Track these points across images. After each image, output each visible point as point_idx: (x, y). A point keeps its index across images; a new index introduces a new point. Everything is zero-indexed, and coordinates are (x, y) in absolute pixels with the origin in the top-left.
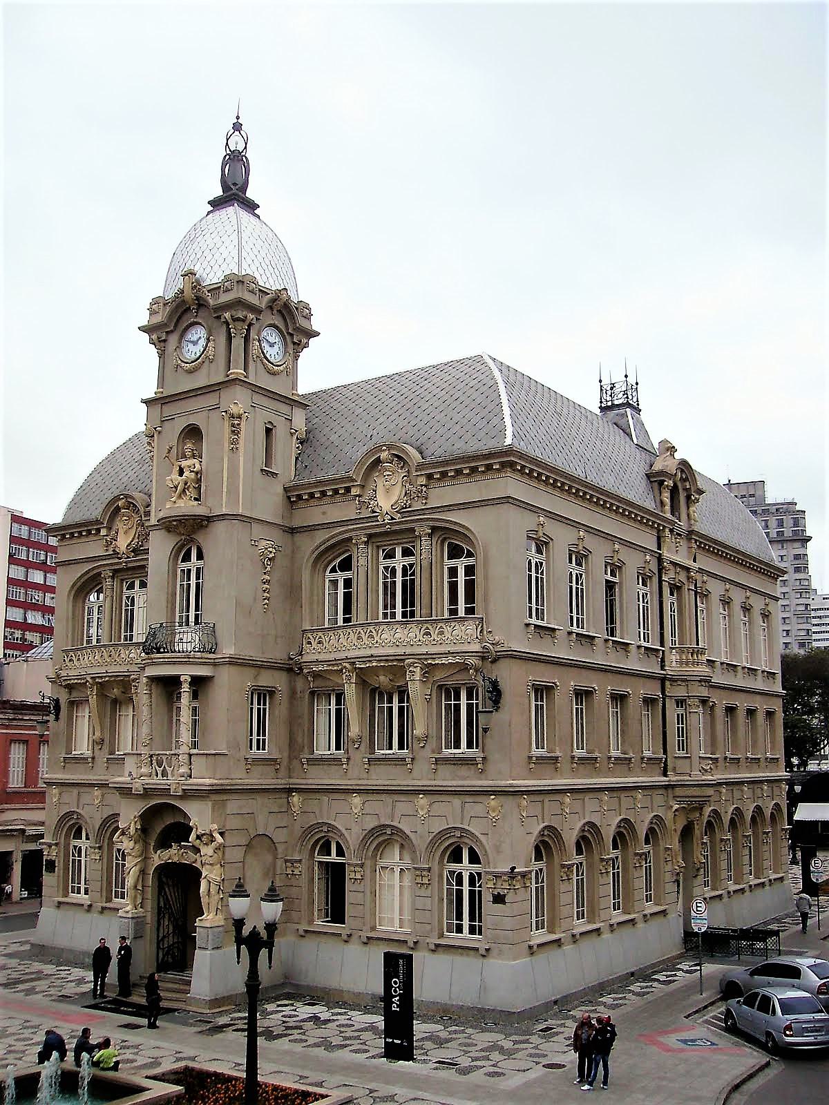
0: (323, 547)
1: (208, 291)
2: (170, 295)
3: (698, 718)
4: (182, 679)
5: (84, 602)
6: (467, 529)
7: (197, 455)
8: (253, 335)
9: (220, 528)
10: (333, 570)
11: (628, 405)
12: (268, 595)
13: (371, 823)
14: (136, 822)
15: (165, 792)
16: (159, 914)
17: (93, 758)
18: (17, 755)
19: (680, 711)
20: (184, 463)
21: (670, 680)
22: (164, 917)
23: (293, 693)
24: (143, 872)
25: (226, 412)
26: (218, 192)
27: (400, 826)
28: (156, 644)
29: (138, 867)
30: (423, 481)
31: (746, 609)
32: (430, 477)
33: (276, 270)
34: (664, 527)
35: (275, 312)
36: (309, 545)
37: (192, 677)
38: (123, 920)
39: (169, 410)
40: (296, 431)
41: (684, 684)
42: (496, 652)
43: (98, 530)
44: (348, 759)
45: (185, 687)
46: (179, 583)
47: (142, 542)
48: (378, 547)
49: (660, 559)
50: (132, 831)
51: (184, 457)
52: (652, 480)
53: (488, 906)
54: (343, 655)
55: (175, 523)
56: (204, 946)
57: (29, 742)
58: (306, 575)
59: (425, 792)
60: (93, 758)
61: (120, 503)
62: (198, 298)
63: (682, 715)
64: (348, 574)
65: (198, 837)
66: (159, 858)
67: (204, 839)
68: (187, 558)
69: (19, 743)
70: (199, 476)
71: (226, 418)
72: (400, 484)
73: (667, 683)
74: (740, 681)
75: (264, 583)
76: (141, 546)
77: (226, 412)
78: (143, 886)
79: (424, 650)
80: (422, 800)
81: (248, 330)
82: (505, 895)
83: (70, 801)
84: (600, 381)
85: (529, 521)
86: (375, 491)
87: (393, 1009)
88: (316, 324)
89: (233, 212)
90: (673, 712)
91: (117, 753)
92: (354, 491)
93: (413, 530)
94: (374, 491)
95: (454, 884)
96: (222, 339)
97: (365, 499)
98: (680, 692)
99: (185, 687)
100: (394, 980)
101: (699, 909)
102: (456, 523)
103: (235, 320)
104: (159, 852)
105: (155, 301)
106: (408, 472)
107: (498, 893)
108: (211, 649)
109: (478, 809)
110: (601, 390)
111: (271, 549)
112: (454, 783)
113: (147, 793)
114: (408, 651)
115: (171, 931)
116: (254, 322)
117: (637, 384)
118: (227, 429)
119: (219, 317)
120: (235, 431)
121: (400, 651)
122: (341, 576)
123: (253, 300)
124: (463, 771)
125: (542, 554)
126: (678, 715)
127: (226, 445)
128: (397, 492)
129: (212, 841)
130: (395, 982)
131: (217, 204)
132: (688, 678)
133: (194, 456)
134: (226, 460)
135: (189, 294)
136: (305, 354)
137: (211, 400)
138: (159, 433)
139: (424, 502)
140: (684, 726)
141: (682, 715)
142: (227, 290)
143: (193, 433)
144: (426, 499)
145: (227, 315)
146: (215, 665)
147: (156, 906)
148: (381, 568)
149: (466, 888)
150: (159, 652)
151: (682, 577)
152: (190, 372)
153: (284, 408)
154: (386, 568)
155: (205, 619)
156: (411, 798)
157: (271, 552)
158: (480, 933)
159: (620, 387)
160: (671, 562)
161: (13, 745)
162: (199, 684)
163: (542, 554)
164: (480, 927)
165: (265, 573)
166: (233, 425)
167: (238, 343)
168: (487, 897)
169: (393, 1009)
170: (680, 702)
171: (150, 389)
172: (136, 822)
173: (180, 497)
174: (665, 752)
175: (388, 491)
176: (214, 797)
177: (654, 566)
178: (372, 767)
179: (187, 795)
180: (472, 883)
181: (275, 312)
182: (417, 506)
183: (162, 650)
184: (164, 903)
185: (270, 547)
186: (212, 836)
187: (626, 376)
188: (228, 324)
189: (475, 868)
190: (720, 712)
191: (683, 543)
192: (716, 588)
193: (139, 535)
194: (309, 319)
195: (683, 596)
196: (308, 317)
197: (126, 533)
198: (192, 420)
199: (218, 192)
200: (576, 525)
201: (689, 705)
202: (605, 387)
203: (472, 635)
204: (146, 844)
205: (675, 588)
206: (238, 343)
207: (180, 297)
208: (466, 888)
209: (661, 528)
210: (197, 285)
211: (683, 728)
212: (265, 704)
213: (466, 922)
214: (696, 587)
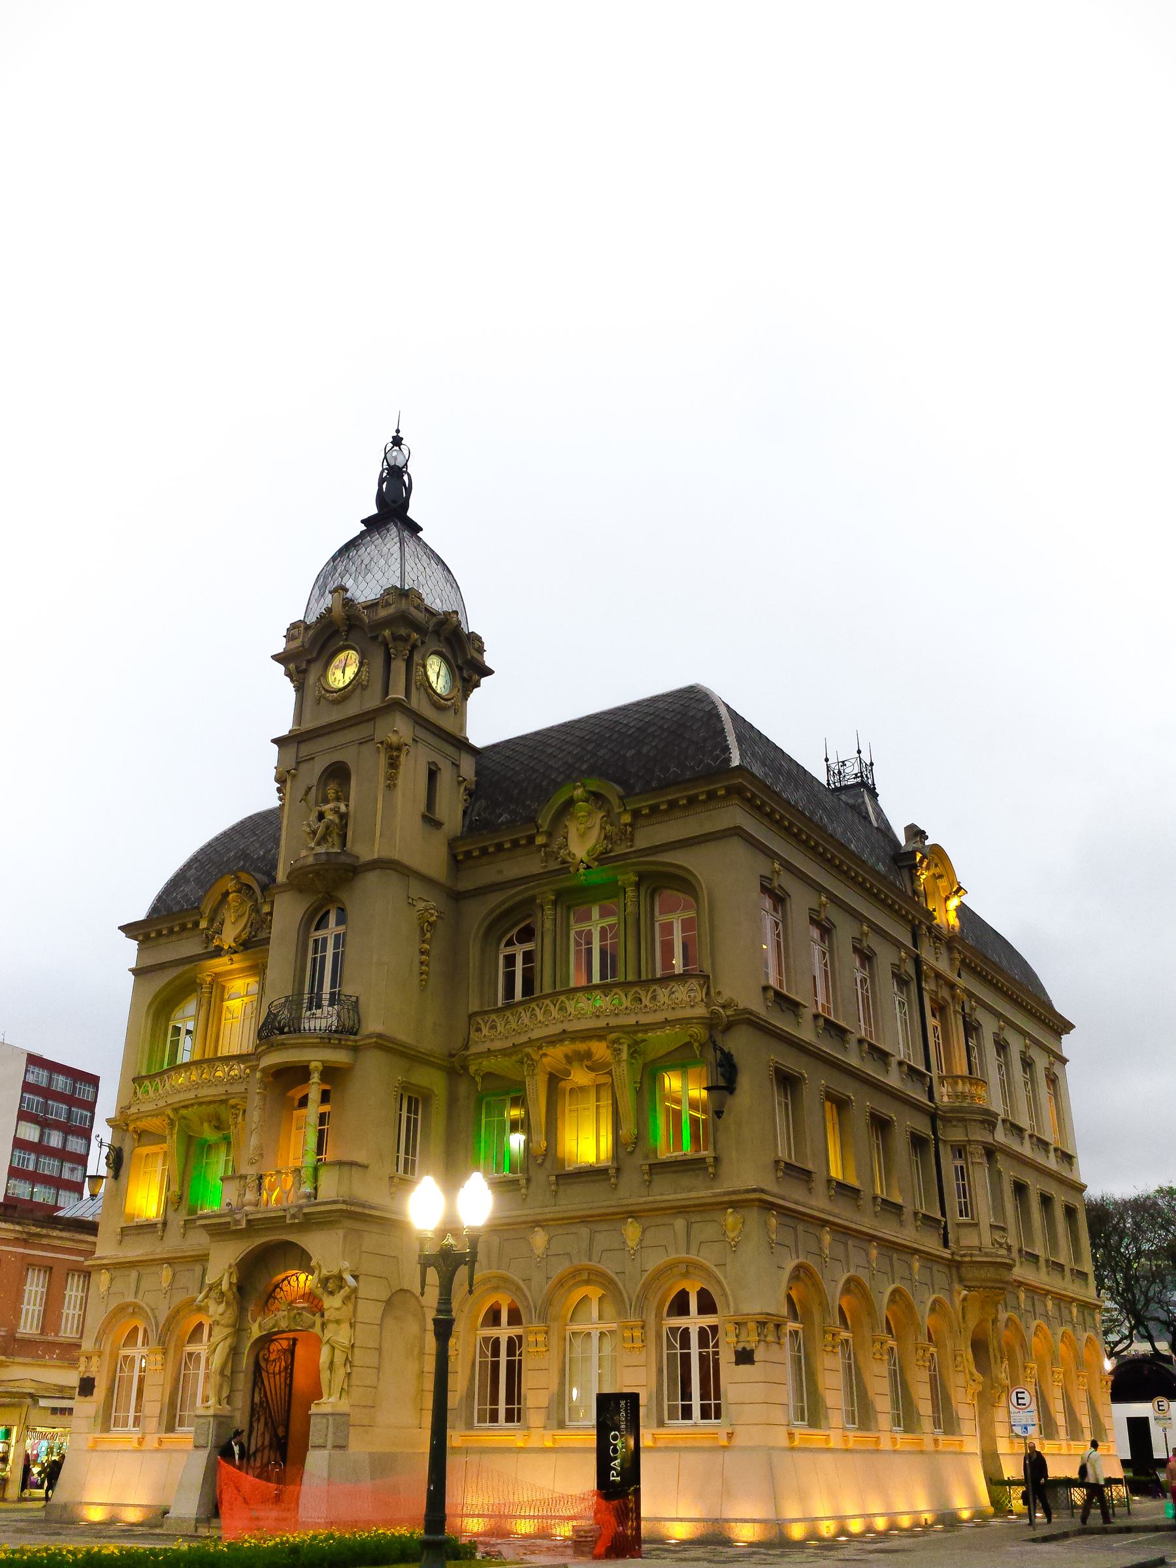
0: (498, 912)
1: (364, 608)
2: (312, 619)
3: (980, 1177)
4: (313, 1065)
5: (168, 1020)
8: (417, 658)
9: (371, 879)
10: (510, 943)
11: (863, 784)
12: (427, 969)
14: (231, 1274)
16: (252, 1415)
17: (165, 1224)
18: (35, 1287)
19: (959, 1163)
20: (326, 808)
21: (944, 1119)
22: (259, 1420)
23: (452, 1101)
24: (234, 1352)
25: (382, 743)
26: (374, 511)
27: (603, 1267)
28: (279, 1022)
29: (229, 1341)
30: (627, 819)
31: (1027, 1064)
32: (636, 814)
33: (444, 592)
34: (921, 922)
35: (442, 638)
36: (478, 913)
37: (323, 1062)
38: (202, 1420)
39: (306, 749)
40: (465, 780)
41: (960, 1124)
42: (728, 1016)
43: (196, 924)
44: (528, 1180)
45: (315, 1078)
46: (310, 956)
47: (256, 932)
48: (569, 908)
49: (918, 962)
50: (225, 1286)
51: (326, 801)
52: (900, 864)
53: (730, 1373)
54: (523, 1039)
55: (311, 876)
56: (320, 1442)
57: (54, 1270)
58: (474, 952)
60: (165, 1224)
62: (349, 618)
63: (962, 1167)
64: (528, 947)
67: (331, 1285)
68: (322, 924)
69: (39, 1270)
70: (344, 821)
71: (382, 750)
72: (597, 827)
73: (939, 1123)
74: (1026, 1149)
75: (422, 953)
76: (254, 936)
77: (382, 743)
78: (232, 1373)
79: (631, 1020)
81: (411, 653)
82: (752, 1352)
83: (125, 1289)
84: (827, 760)
85: (763, 866)
86: (566, 838)
87: (612, 1478)
88: (489, 660)
89: (390, 541)
90: (949, 1164)
91: (200, 1212)
92: (540, 840)
94: (564, 838)
95: (678, 1346)
96: (378, 662)
97: (555, 847)
98: (956, 1135)
99: (315, 1078)
100: (613, 1433)
101: (1020, 1401)
103: (395, 638)
104: (259, 1319)
105: (294, 626)
106: (608, 812)
107: (744, 1348)
108: (352, 1028)
109: (708, 1231)
110: (828, 771)
111: (432, 911)
112: (679, 1196)
113: (253, 1226)
114: (613, 1022)
115: (267, 1442)
116: (419, 643)
117: (872, 764)
118: (383, 760)
119: (375, 638)
120: (393, 764)
121: (601, 1023)
122: (519, 950)
123: (420, 616)
124: (685, 1180)
125: (778, 913)
126: (956, 1167)
127: (382, 779)
128: (595, 834)
129: (341, 1287)
130: (615, 1438)
131: (372, 524)
132: (968, 1116)
133: (338, 799)
134: (380, 798)
136: (476, 696)
139: (629, 844)
140: (966, 1182)
141: (962, 1167)
142: (388, 604)
143: (338, 774)
144: (632, 840)
145: (387, 633)
146: (355, 1049)
147: (249, 1402)
148: (572, 934)
149: (695, 1351)
150: (282, 1033)
151: (945, 993)
152: (336, 702)
153: (449, 749)
154: (579, 934)
155: (348, 989)
157: (432, 915)
158: (718, 1417)
159: (852, 769)
160: (932, 968)
161: (30, 1270)
162: (331, 1073)
163: (778, 913)
164: (718, 1407)
165: (424, 942)
166: (391, 758)
167: (399, 666)
168: (726, 1357)
169: (612, 1478)
170: (960, 1151)
171: (285, 726)
172: (231, 1274)
173: (318, 844)
174: (944, 1214)
175: (583, 836)
176: (348, 1223)
177: (910, 968)
178: (562, 1187)
179: (311, 1221)
180: (703, 1343)
181: (442, 638)
183: (286, 1030)
184: (261, 1398)
185: (431, 908)
186: (341, 1279)
187: (859, 752)
188: (386, 645)
189: (708, 1320)
190: (1008, 1189)
191: (943, 950)
192: (989, 1027)
193: (252, 923)
194: (482, 654)
195: (949, 1019)
196: (481, 650)
197: (234, 923)
198: (337, 757)
199: (374, 511)
200: (819, 889)
201: (971, 1154)
202: (833, 766)
203: (695, 997)
204: (242, 1311)
205: (940, 1009)
206: (399, 666)
207: (326, 620)
208: (695, 1351)
209: (917, 923)
210: (348, 603)
211: (964, 1185)
212: (416, 1113)
213: (696, 1403)
214: (963, 1009)
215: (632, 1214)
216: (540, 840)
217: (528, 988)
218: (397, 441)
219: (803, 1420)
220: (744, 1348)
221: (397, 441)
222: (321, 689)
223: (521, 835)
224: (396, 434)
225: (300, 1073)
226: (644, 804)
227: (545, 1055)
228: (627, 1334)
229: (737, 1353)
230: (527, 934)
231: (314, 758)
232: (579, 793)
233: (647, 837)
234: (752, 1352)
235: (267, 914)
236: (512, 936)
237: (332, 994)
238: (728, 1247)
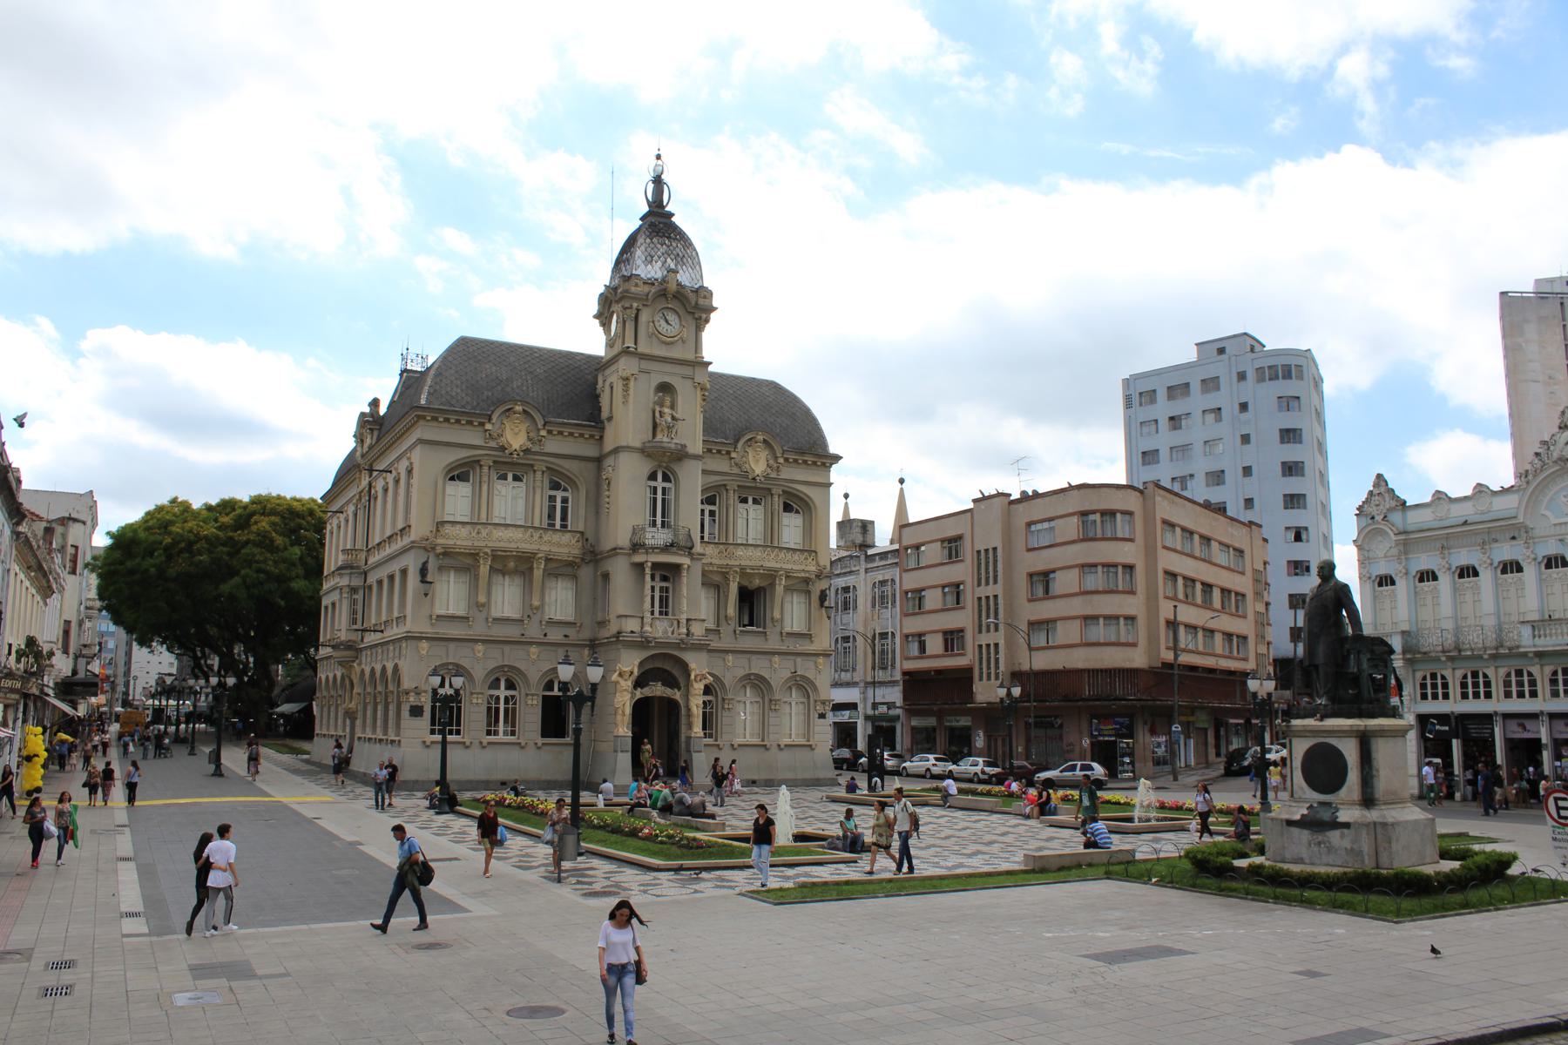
6: (808, 497)
7: (672, 407)
9: (693, 462)
13: (741, 673)
15: (677, 646)
43: (482, 424)
59: (780, 654)
61: (519, 408)
62: (678, 292)
64: (712, 508)
65: (696, 677)
66: (639, 694)
71: (699, 389)
79: (789, 566)
80: (776, 658)
92: (733, 455)
93: (769, 490)
102: (805, 494)
109: (811, 664)
121: (778, 566)
122: (708, 508)
135: (672, 287)
137: (687, 371)
138: (636, 379)
146: (692, 559)
156: (768, 657)
175: (758, 461)
182: (773, 475)
198: (667, 379)
215: (780, 654)
216: (733, 455)
218: (658, 157)
221: (658, 157)
223: (724, 449)
224: (657, 152)
225: (676, 568)
226: (792, 457)
232: (760, 438)
233: (788, 473)
237: (663, 522)
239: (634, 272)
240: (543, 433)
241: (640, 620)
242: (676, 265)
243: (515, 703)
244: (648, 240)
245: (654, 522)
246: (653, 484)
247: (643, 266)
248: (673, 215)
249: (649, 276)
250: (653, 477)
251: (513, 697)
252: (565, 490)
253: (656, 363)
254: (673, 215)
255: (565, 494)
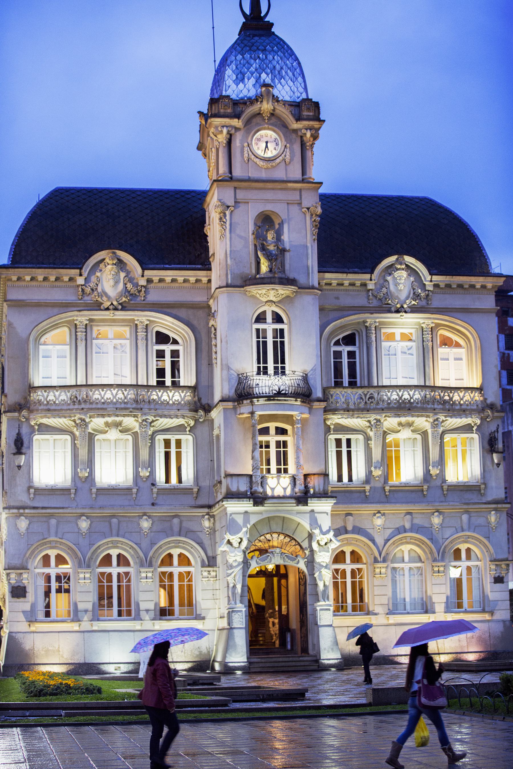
10: (337, 343)
64: (350, 348)
82: (503, 578)
122: (345, 349)
144: (431, 300)
198: (269, 207)
217: (352, 374)
219: (480, 607)
220: (499, 576)
222: (250, 153)
227: (386, 420)
228: (436, 569)
229: (495, 578)
230: (349, 340)
231: (248, 202)
234: (503, 578)
235: (142, 286)
236: (339, 339)
238: (490, 529)
239: (224, 93)
240: (142, 282)
241: (248, 479)
242: (273, 80)
243: (129, 581)
244: (239, 57)
245: (265, 368)
246: (261, 326)
247: (233, 86)
248: (272, 25)
249: (241, 96)
250: (261, 318)
251: (127, 574)
252: (175, 342)
253: (256, 192)
254: (272, 25)
255: (175, 347)
